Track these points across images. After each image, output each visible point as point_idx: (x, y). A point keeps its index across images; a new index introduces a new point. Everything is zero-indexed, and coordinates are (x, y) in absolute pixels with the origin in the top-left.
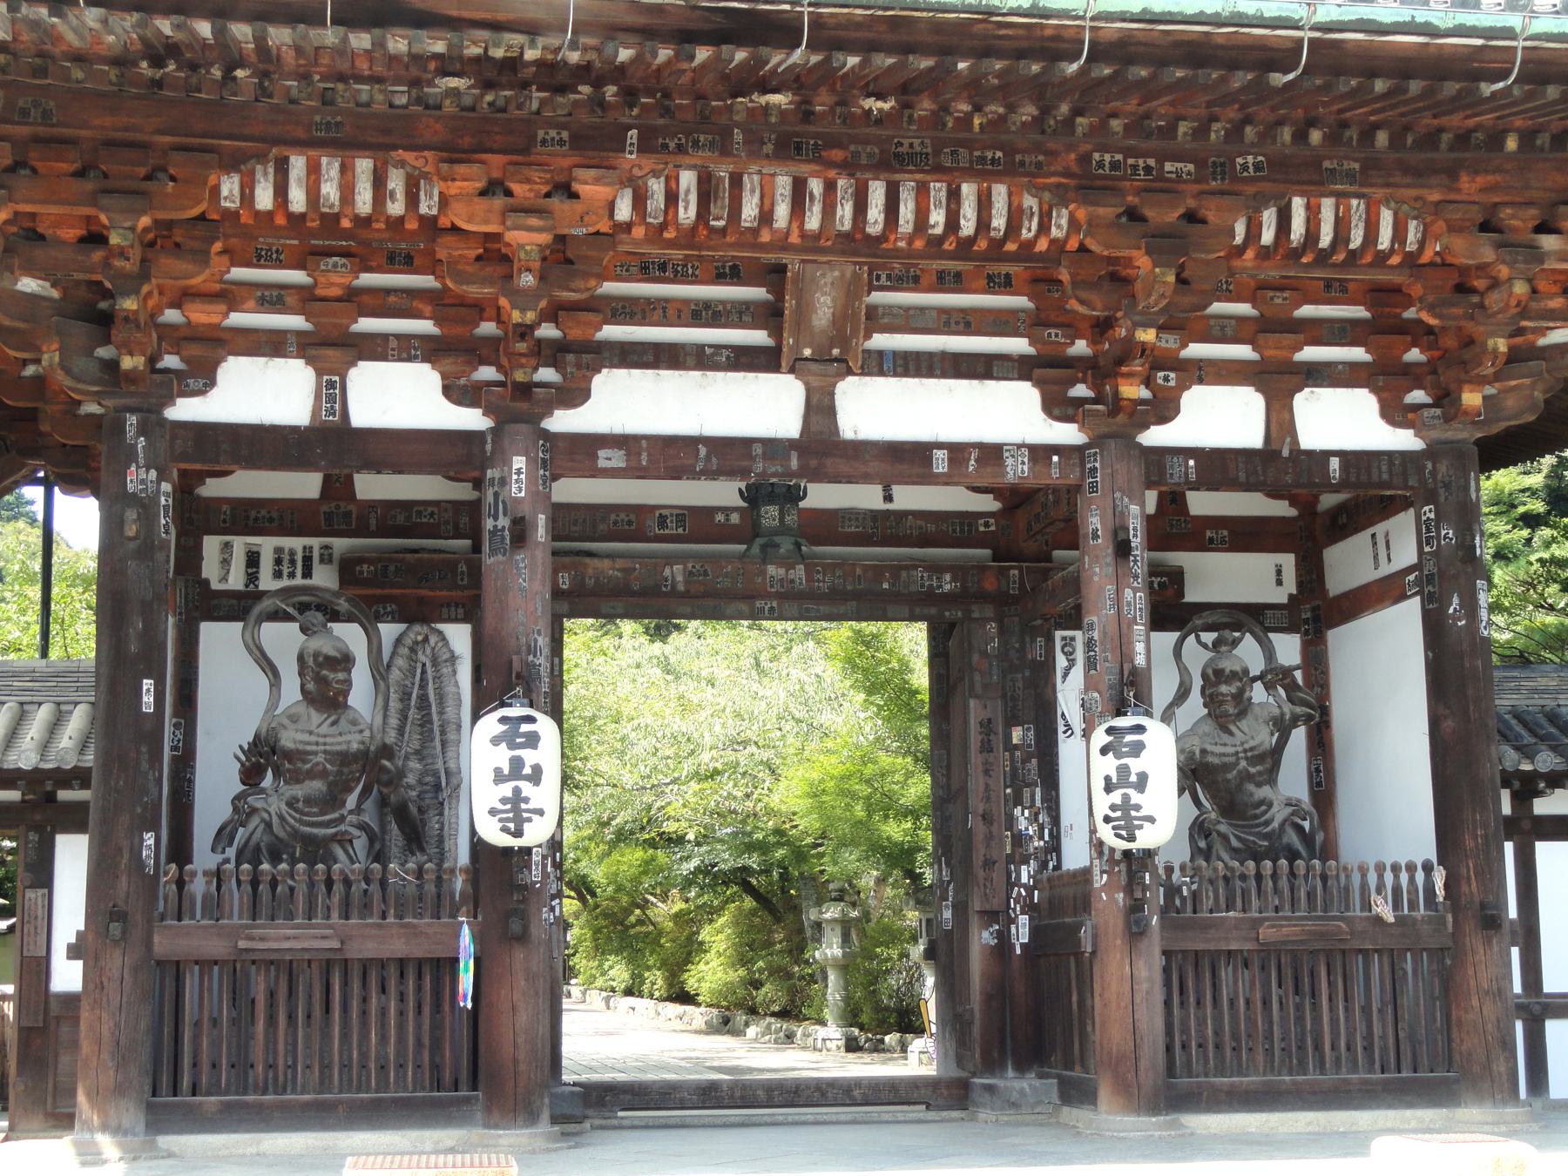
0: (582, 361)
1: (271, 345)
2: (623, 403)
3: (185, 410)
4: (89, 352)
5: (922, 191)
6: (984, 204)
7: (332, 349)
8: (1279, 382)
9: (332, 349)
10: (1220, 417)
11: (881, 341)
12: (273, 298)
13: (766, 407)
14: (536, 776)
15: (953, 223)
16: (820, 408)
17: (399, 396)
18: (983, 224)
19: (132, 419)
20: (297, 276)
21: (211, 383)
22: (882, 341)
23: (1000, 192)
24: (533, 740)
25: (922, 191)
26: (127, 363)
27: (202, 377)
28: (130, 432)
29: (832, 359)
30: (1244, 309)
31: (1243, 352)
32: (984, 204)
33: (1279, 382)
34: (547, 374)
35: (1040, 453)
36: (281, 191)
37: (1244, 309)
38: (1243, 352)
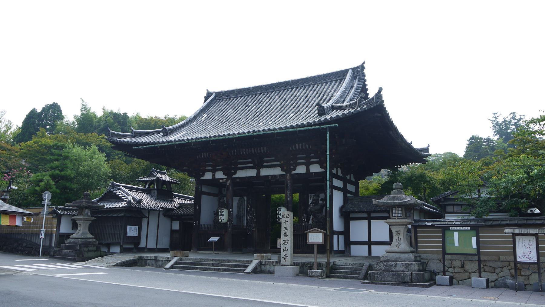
0: (236, 169)
1: (209, 171)
2: (241, 174)
3: (202, 178)
5: (257, 149)
6: (263, 149)
7: (214, 171)
8: (308, 165)
9: (214, 171)
10: (301, 170)
11: (265, 164)
12: (209, 166)
13: (252, 173)
14: (223, 215)
15: (260, 151)
16: (258, 173)
17: (220, 175)
18: (264, 151)
20: (211, 163)
22: (265, 164)
23: (265, 148)
24: (223, 212)
25: (257, 149)
27: (203, 175)
29: (259, 166)
30: (304, 155)
31: (304, 161)
32: (263, 149)
33: (308, 165)
34: (233, 171)
35: (280, 175)
36: (201, 156)
37: (304, 155)
38: (304, 161)
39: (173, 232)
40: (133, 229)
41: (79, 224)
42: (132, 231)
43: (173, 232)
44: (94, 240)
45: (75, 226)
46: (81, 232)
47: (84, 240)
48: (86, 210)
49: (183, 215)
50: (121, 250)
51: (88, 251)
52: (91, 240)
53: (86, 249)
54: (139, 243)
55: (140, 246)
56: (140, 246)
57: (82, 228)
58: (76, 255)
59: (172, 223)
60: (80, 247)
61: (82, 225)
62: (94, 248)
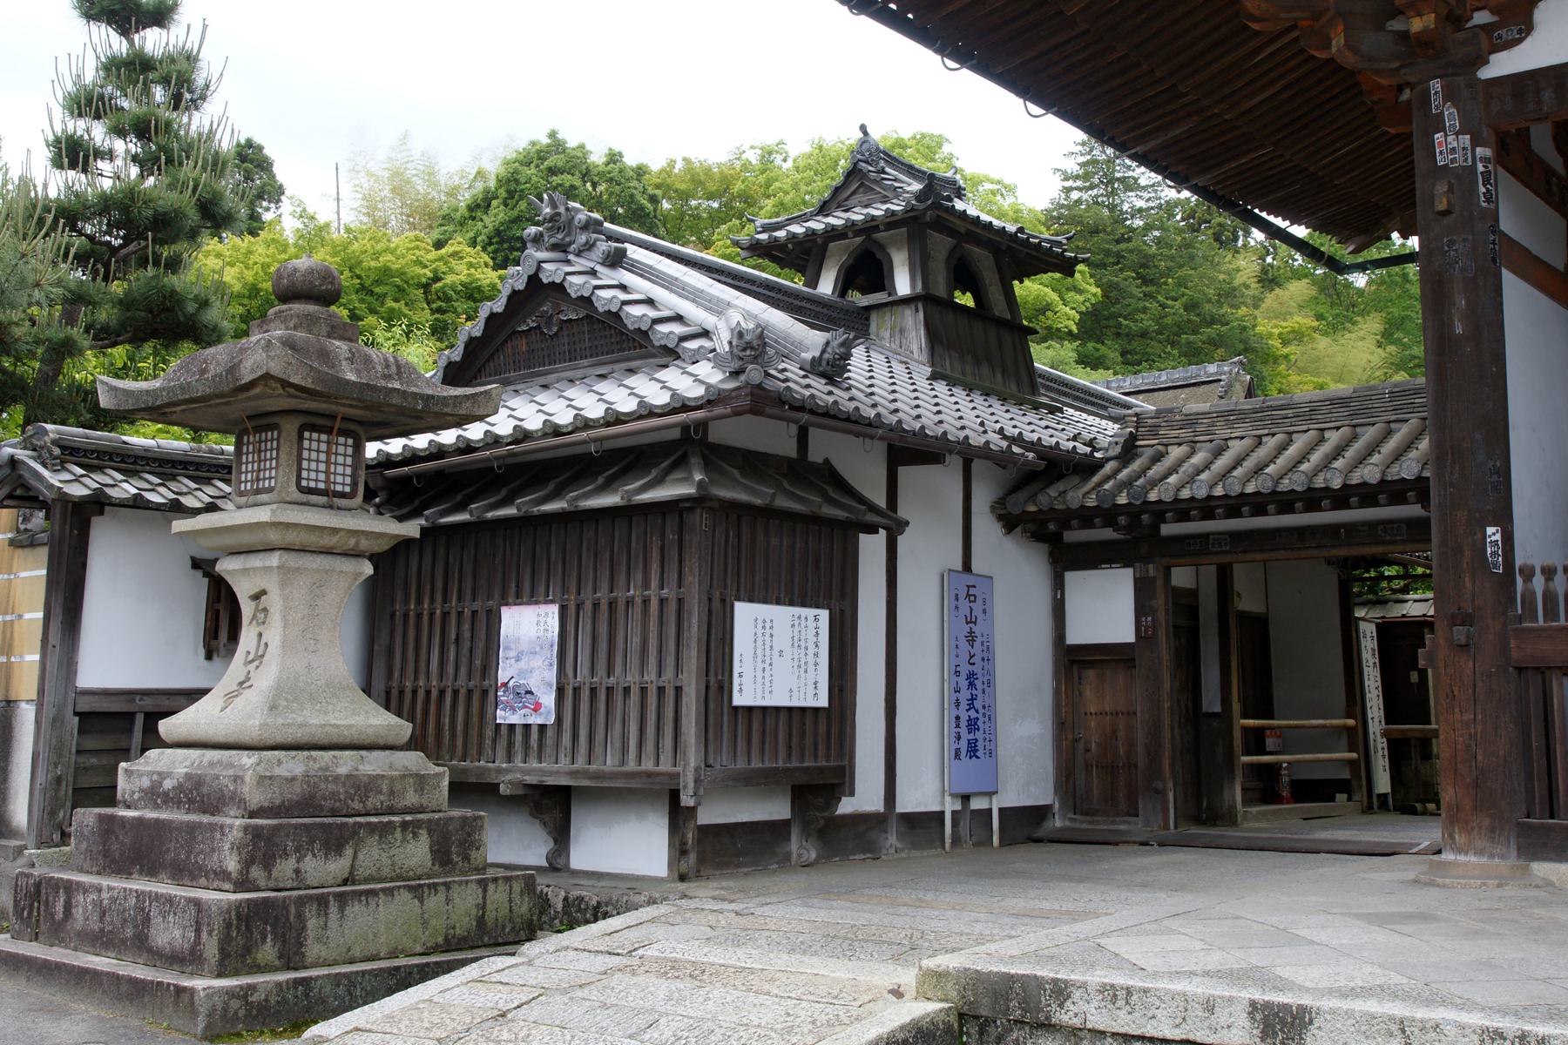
4: (1381, 28)
19: (1436, 85)
21: (1527, 28)
26: (1417, 25)
28: (1436, 101)
39: (1075, 662)
40: (782, 639)
41: (243, 590)
42: (775, 655)
43: (1075, 662)
44: (414, 760)
45: (222, 622)
46: (266, 678)
47: (293, 765)
48: (315, 443)
49: (1183, 509)
50: (678, 850)
51: (351, 891)
52: (374, 764)
53: (323, 869)
54: (840, 780)
55: (846, 806)
56: (846, 806)
57: (274, 635)
58: (211, 948)
59: (1058, 585)
60: (262, 848)
61: (274, 601)
62: (417, 853)
